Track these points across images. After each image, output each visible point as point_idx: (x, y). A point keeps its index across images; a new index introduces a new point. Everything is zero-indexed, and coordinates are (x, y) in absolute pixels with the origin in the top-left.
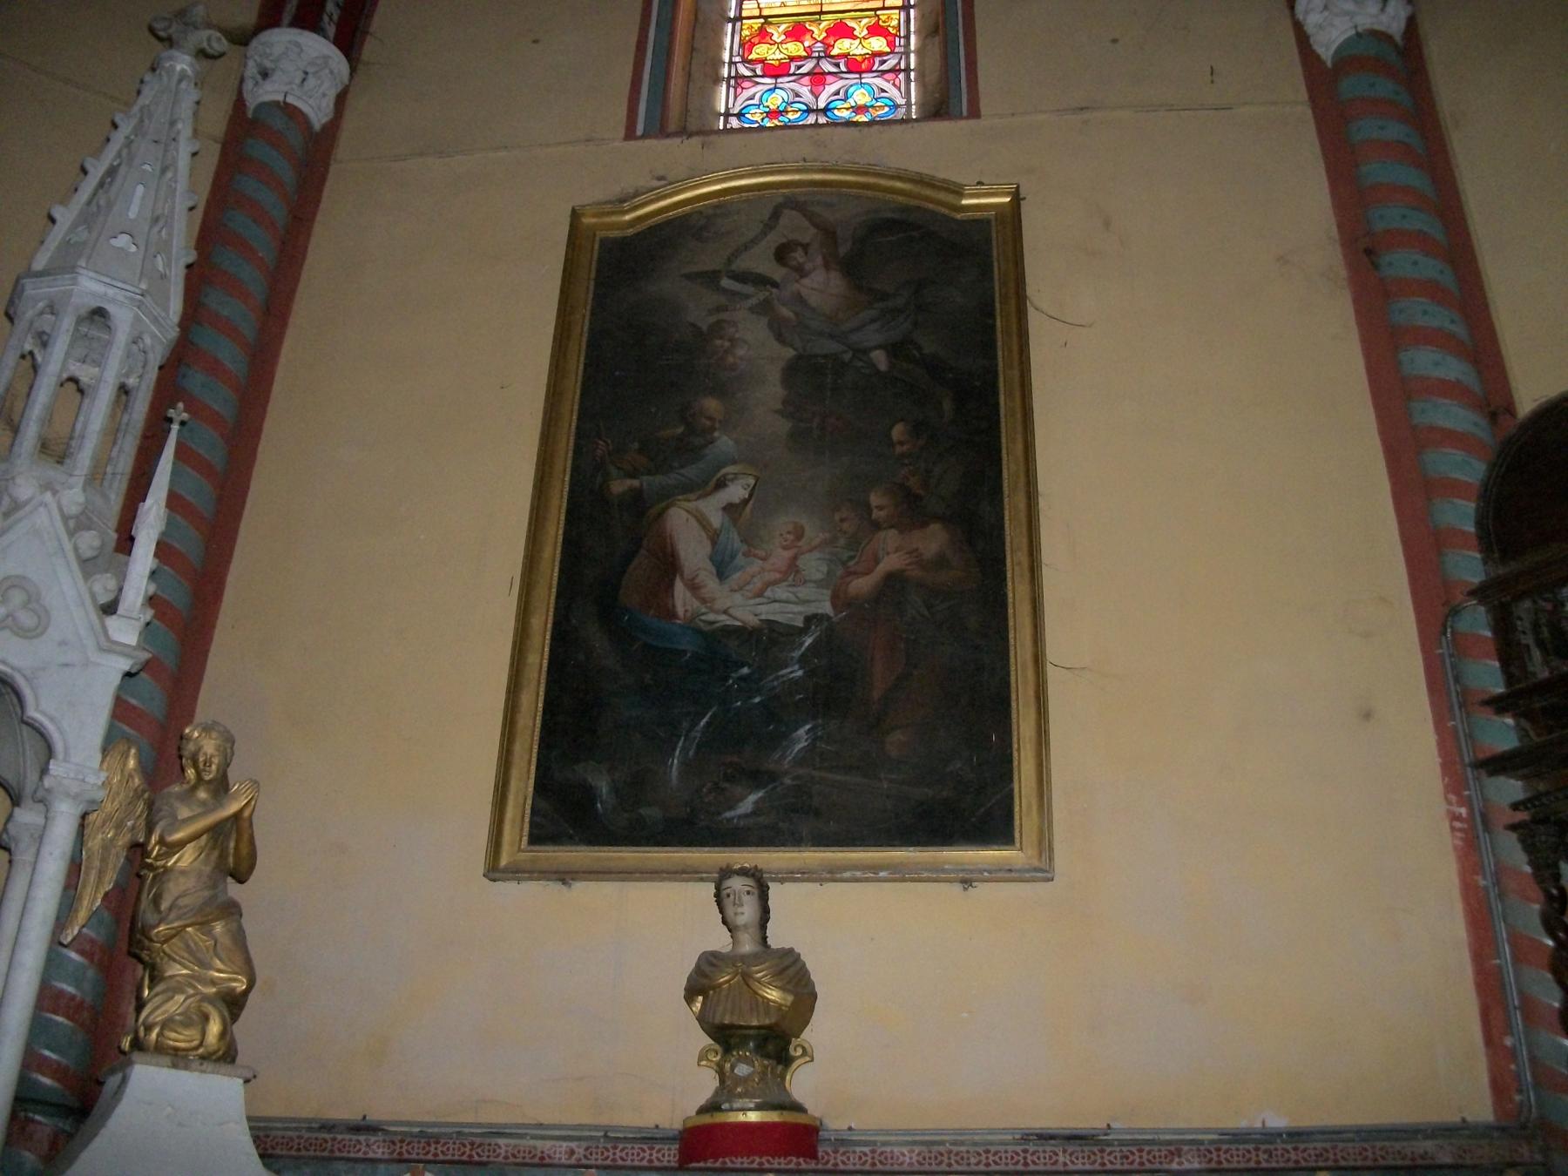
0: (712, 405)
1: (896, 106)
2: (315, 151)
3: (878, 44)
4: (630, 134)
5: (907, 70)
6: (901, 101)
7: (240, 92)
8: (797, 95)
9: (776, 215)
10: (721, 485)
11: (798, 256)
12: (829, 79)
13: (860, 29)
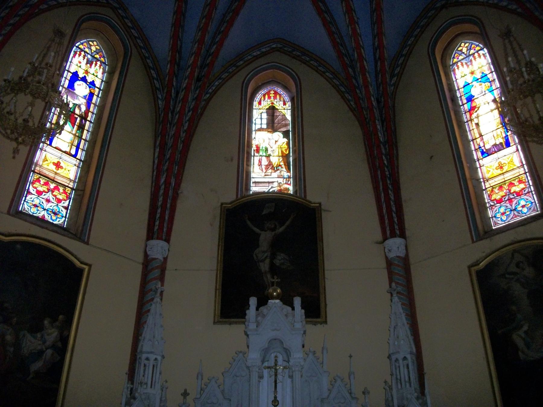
0: (514, 308)
1: (532, 203)
2: (405, 261)
3: (522, 186)
4: (473, 242)
5: (532, 191)
6: (533, 201)
7: (386, 255)
8: (507, 207)
9: (513, 255)
10: (522, 327)
11: (521, 264)
12: (513, 200)
13: (516, 183)
